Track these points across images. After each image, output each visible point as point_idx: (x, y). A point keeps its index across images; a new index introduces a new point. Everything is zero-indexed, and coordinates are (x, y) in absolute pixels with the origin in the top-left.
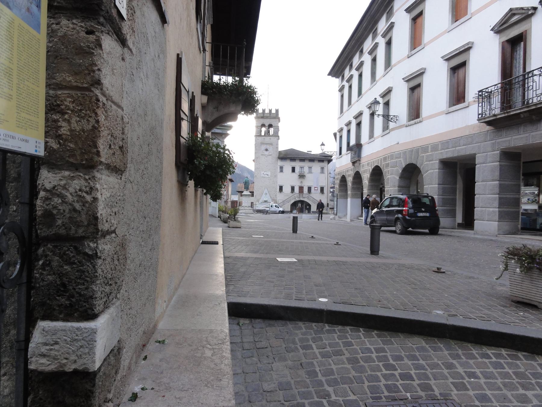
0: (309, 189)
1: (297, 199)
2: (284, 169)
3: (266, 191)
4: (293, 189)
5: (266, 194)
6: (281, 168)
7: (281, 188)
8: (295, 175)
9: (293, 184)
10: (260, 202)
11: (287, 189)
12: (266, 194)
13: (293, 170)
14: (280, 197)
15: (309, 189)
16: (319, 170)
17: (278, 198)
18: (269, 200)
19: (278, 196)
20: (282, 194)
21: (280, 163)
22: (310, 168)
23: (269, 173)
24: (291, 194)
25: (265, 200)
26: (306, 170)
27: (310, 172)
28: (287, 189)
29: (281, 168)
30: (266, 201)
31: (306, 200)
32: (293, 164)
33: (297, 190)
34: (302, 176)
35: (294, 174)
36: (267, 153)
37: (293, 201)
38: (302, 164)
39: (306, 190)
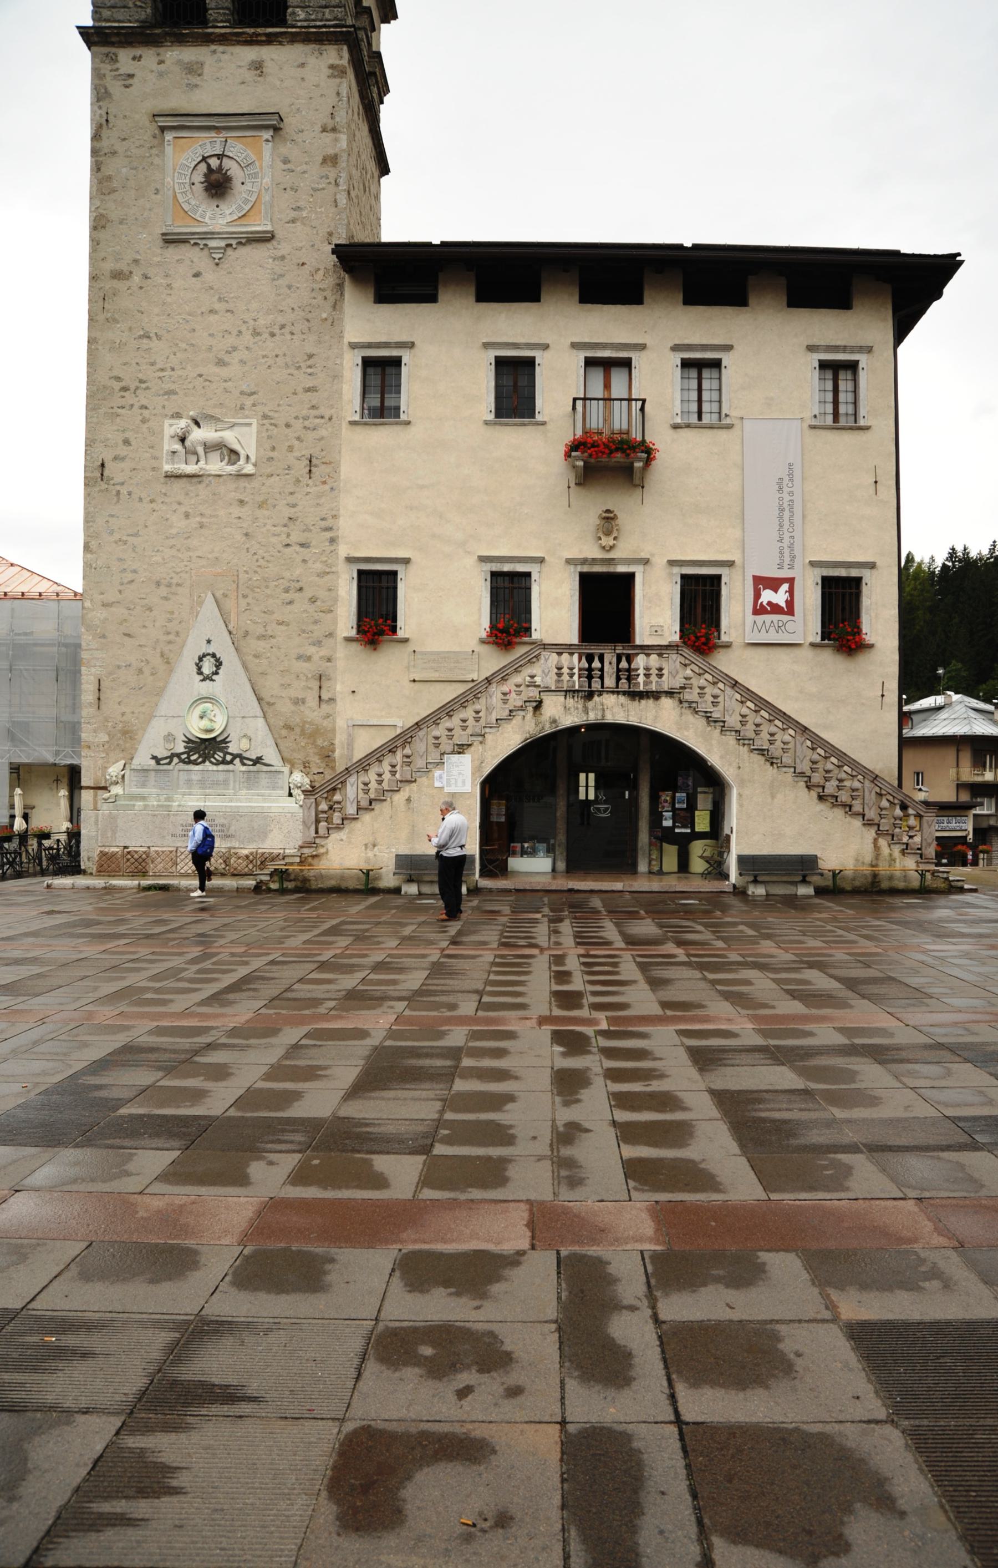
0: (700, 598)
1: (563, 713)
2: (413, 390)
3: (206, 629)
4: (510, 595)
5: (209, 666)
6: (382, 371)
7: (378, 600)
8: (538, 451)
9: (509, 546)
10: (142, 759)
11: (445, 611)
12: (209, 666)
13: (515, 387)
14: (371, 699)
15: (700, 598)
16: (806, 389)
17: (347, 712)
18: (250, 735)
19: (340, 687)
20: (390, 660)
21: (368, 323)
22: (700, 366)
23: (245, 438)
24: (493, 661)
25: (196, 728)
26: (658, 382)
27: (701, 417)
28: (445, 611)
29: (382, 371)
30: (207, 749)
31: (663, 718)
32: (514, 326)
33: (555, 611)
34: (609, 461)
35: (515, 437)
36: (219, 218)
37: (507, 741)
38: (609, 326)
39: (656, 613)
